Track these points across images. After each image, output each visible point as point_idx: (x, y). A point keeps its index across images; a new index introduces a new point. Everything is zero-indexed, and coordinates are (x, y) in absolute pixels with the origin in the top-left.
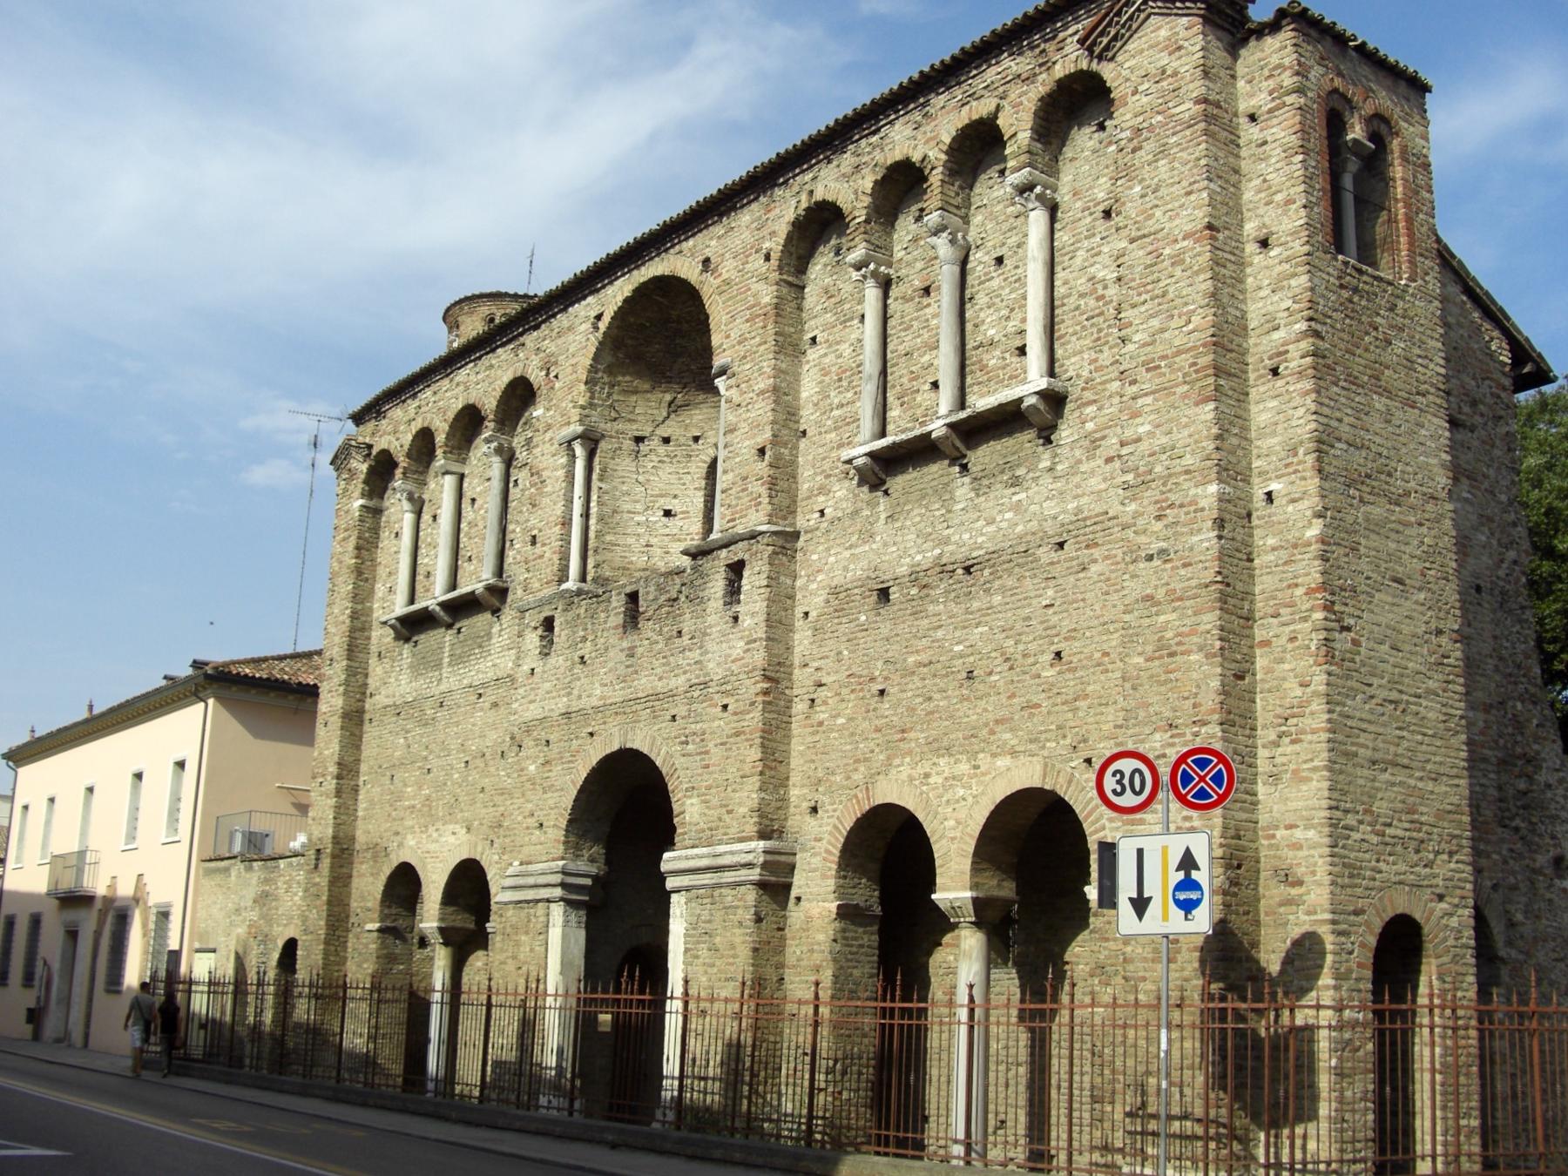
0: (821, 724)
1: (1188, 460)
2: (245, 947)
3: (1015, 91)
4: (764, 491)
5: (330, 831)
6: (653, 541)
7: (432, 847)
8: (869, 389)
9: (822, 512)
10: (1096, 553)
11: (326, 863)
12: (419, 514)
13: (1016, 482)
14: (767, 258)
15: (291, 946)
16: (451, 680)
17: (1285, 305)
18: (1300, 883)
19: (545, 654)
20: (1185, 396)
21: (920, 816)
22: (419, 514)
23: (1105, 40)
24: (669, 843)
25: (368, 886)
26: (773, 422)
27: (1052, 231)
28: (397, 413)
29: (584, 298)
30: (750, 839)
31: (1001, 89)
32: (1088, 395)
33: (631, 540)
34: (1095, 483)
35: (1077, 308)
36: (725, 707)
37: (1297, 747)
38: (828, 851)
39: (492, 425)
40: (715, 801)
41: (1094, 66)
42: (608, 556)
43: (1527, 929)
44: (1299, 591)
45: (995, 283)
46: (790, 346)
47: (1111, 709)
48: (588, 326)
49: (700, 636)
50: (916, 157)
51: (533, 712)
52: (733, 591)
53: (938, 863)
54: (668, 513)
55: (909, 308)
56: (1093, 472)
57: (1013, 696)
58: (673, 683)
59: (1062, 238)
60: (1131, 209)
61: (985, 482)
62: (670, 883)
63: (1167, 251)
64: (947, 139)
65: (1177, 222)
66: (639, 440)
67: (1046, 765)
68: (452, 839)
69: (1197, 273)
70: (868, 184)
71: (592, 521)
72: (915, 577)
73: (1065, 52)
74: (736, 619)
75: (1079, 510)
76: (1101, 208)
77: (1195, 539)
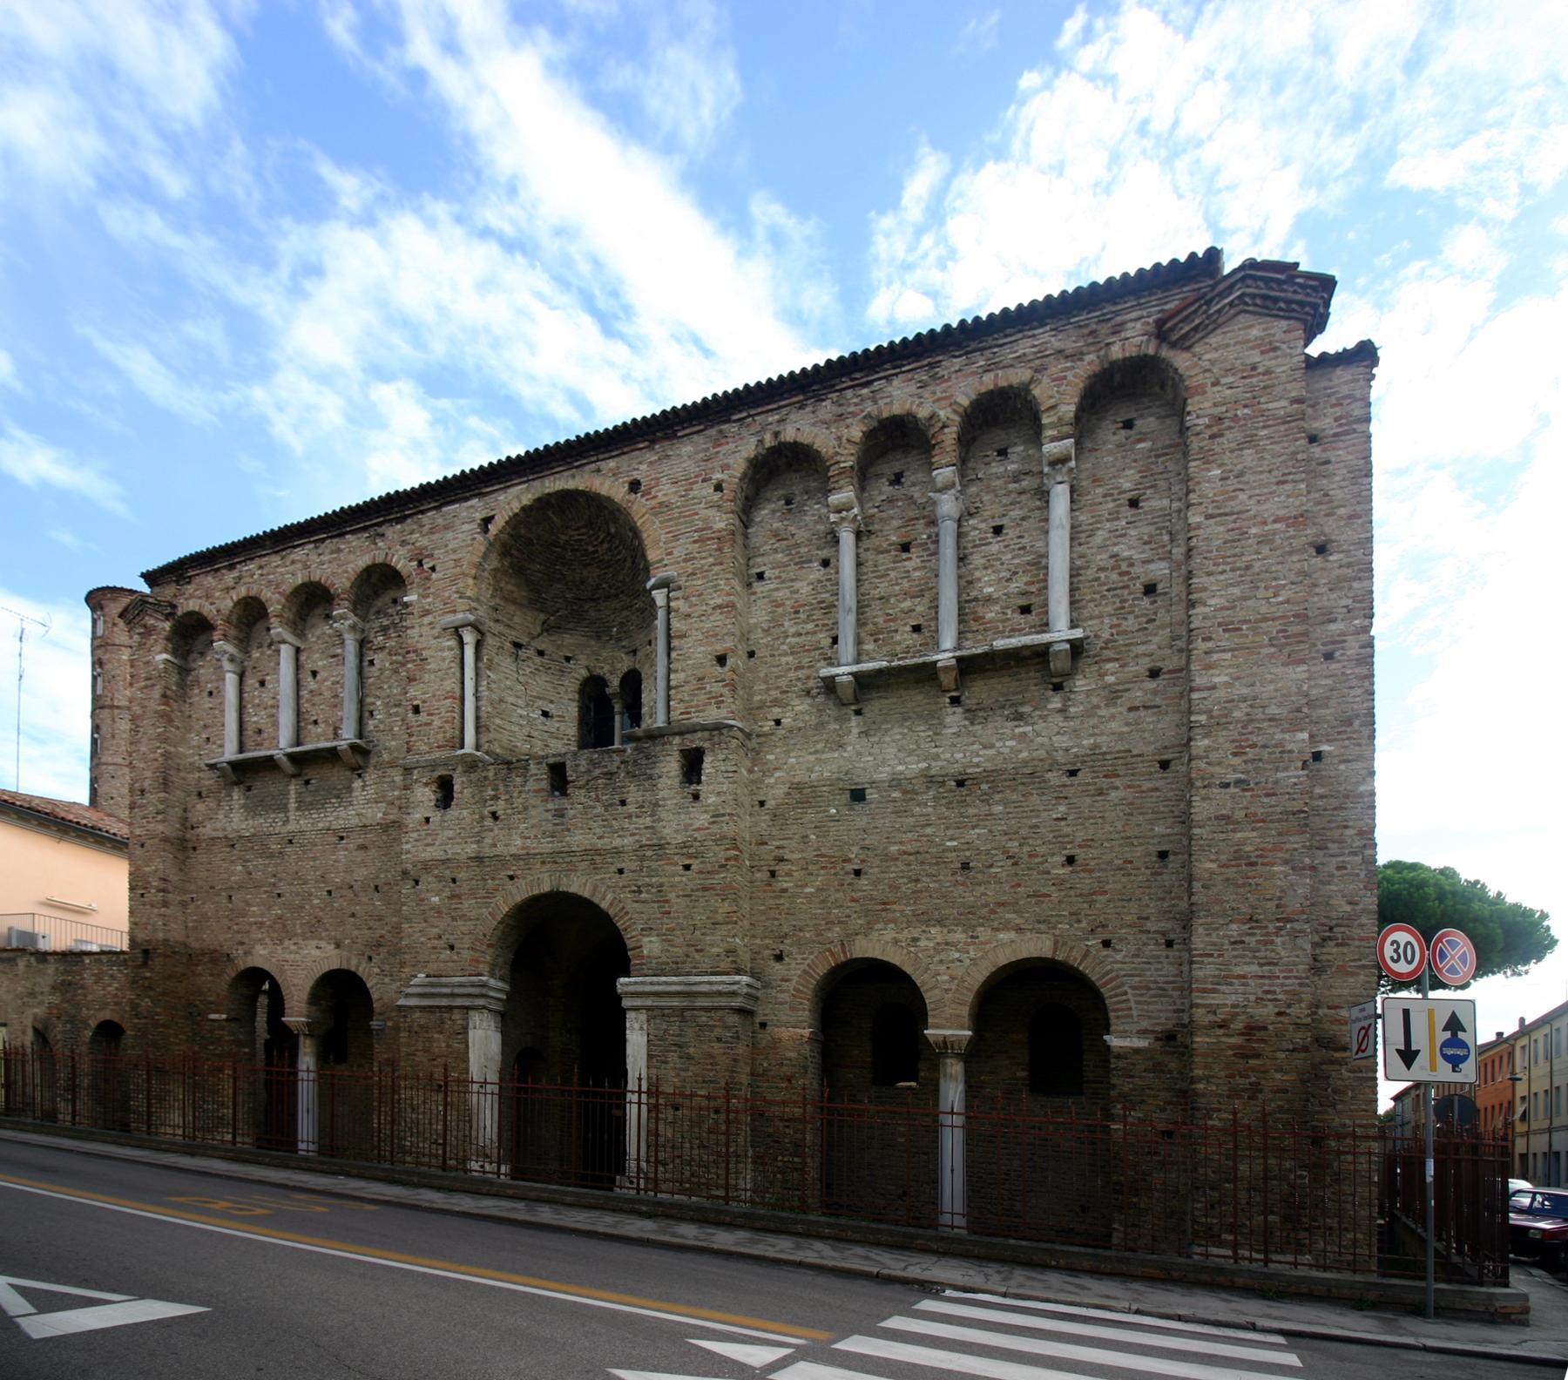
3: (1056, 367)
10: (1118, 782)
13: (1019, 717)
17: (1344, 602)
23: (1187, 328)
31: (1038, 362)
37: (1344, 950)
41: (1165, 353)
45: (994, 548)
56: (1113, 717)
64: (965, 402)
72: (896, 782)
73: (1123, 335)
75: (1095, 746)
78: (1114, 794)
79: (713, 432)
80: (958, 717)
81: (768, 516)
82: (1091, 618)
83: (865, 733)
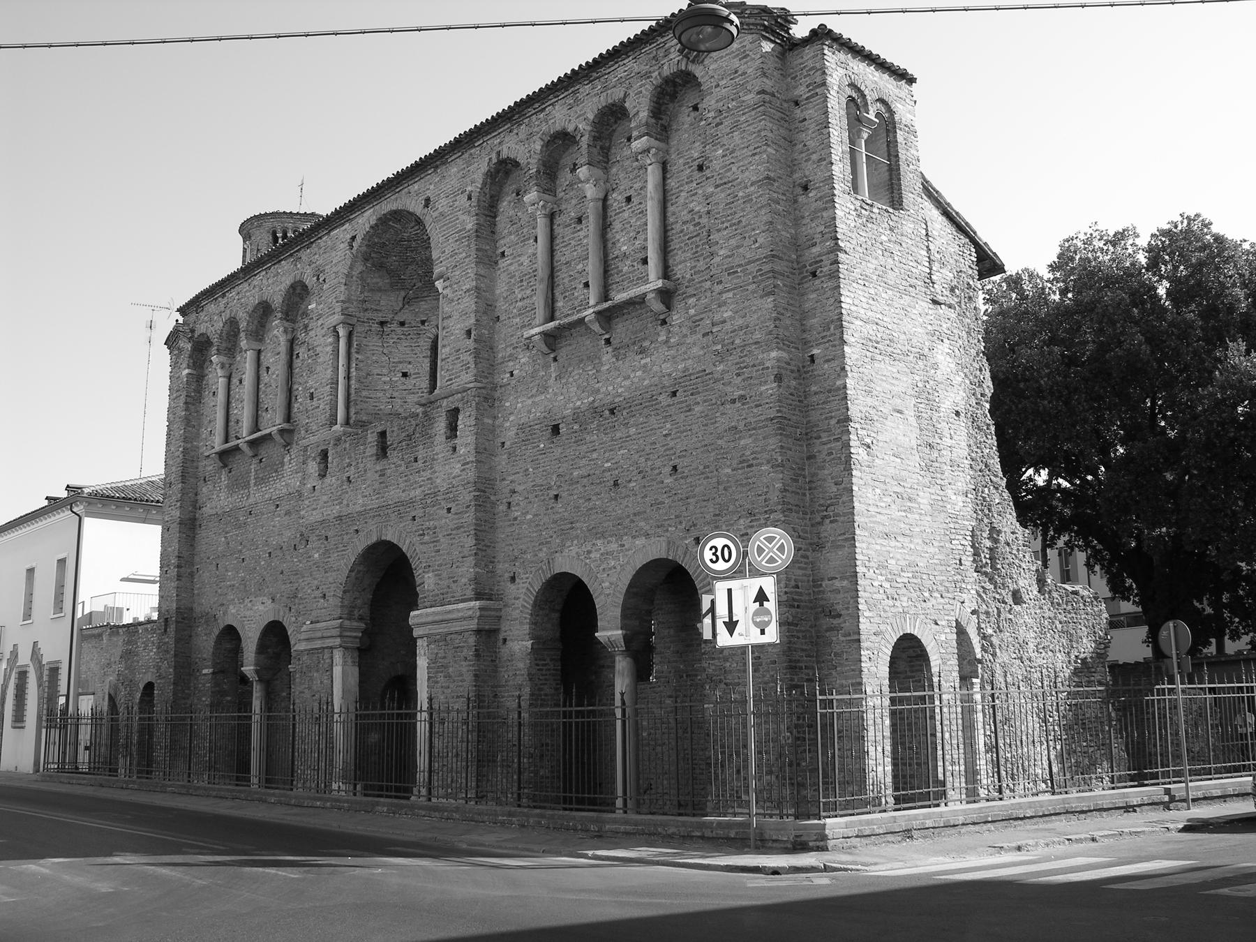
0: (515, 519)
1: (757, 336)
2: (116, 688)
4: (470, 359)
5: (174, 605)
6: (395, 394)
7: (248, 613)
8: (541, 288)
9: (512, 375)
11: (172, 628)
12: (229, 378)
13: (642, 351)
14: (470, 198)
15: (149, 687)
16: (257, 495)
18: (839, 616)
19: (322, 476)
20: (754, 292)
21: (585, 580)
22: (229, 378)
24: (414, 606)
25: (205, 642)
26: (476, 312)
27: (664, 179)
28: (211, 308)
29: (343, 224)
30: (470, 600)
32: (691, 291)
33: (380, 394)
34: (696, 351)
35: (682, 231)
36: (449, 510)
38: (523, 606)
39: (279, 315)
40: (445, 575)
41: (692, 67)
42: (365, 405)
43: (995, 640)
44: (833, 422)
45: (626, 215)
46: (489, 258)
47: (710, 504)
48: (344, 246)
49: (430, 462)
50: (570, 129)
51: (315, 516)
52: (453, 428)
53: (598, 612)
54: (405, 375)
55: (568, 230)
57: (646, 496)
58: (412, 494)
59: (672, 183)
60: (716, 165)
61: (622, 351)
62: (415, 634)
63: (741, 194)
64: (591, 116)
65: (747, 173)
66: (382, 324)
67: (669, 543)
68: (261, 608)
69: (760, 208)
70: (538, 146)
71: (353, 382)
72: (577, 416)
74: (454, 449)
76: (696, 163)
77: (763, 388)
78: (697, 409)
79: (466, 155)
80: (609, 356)
81: (506, 206)
82: (680, 263)
83: (559, 378)
